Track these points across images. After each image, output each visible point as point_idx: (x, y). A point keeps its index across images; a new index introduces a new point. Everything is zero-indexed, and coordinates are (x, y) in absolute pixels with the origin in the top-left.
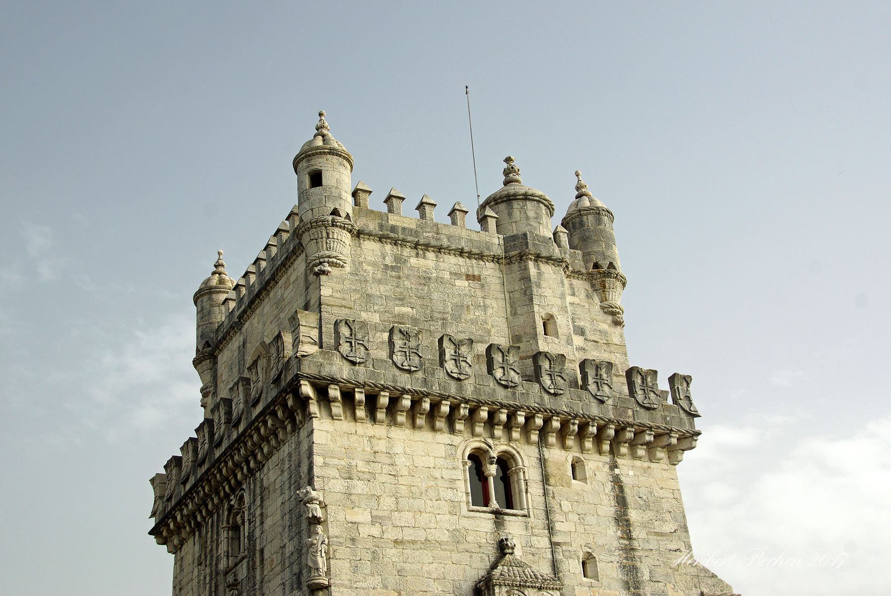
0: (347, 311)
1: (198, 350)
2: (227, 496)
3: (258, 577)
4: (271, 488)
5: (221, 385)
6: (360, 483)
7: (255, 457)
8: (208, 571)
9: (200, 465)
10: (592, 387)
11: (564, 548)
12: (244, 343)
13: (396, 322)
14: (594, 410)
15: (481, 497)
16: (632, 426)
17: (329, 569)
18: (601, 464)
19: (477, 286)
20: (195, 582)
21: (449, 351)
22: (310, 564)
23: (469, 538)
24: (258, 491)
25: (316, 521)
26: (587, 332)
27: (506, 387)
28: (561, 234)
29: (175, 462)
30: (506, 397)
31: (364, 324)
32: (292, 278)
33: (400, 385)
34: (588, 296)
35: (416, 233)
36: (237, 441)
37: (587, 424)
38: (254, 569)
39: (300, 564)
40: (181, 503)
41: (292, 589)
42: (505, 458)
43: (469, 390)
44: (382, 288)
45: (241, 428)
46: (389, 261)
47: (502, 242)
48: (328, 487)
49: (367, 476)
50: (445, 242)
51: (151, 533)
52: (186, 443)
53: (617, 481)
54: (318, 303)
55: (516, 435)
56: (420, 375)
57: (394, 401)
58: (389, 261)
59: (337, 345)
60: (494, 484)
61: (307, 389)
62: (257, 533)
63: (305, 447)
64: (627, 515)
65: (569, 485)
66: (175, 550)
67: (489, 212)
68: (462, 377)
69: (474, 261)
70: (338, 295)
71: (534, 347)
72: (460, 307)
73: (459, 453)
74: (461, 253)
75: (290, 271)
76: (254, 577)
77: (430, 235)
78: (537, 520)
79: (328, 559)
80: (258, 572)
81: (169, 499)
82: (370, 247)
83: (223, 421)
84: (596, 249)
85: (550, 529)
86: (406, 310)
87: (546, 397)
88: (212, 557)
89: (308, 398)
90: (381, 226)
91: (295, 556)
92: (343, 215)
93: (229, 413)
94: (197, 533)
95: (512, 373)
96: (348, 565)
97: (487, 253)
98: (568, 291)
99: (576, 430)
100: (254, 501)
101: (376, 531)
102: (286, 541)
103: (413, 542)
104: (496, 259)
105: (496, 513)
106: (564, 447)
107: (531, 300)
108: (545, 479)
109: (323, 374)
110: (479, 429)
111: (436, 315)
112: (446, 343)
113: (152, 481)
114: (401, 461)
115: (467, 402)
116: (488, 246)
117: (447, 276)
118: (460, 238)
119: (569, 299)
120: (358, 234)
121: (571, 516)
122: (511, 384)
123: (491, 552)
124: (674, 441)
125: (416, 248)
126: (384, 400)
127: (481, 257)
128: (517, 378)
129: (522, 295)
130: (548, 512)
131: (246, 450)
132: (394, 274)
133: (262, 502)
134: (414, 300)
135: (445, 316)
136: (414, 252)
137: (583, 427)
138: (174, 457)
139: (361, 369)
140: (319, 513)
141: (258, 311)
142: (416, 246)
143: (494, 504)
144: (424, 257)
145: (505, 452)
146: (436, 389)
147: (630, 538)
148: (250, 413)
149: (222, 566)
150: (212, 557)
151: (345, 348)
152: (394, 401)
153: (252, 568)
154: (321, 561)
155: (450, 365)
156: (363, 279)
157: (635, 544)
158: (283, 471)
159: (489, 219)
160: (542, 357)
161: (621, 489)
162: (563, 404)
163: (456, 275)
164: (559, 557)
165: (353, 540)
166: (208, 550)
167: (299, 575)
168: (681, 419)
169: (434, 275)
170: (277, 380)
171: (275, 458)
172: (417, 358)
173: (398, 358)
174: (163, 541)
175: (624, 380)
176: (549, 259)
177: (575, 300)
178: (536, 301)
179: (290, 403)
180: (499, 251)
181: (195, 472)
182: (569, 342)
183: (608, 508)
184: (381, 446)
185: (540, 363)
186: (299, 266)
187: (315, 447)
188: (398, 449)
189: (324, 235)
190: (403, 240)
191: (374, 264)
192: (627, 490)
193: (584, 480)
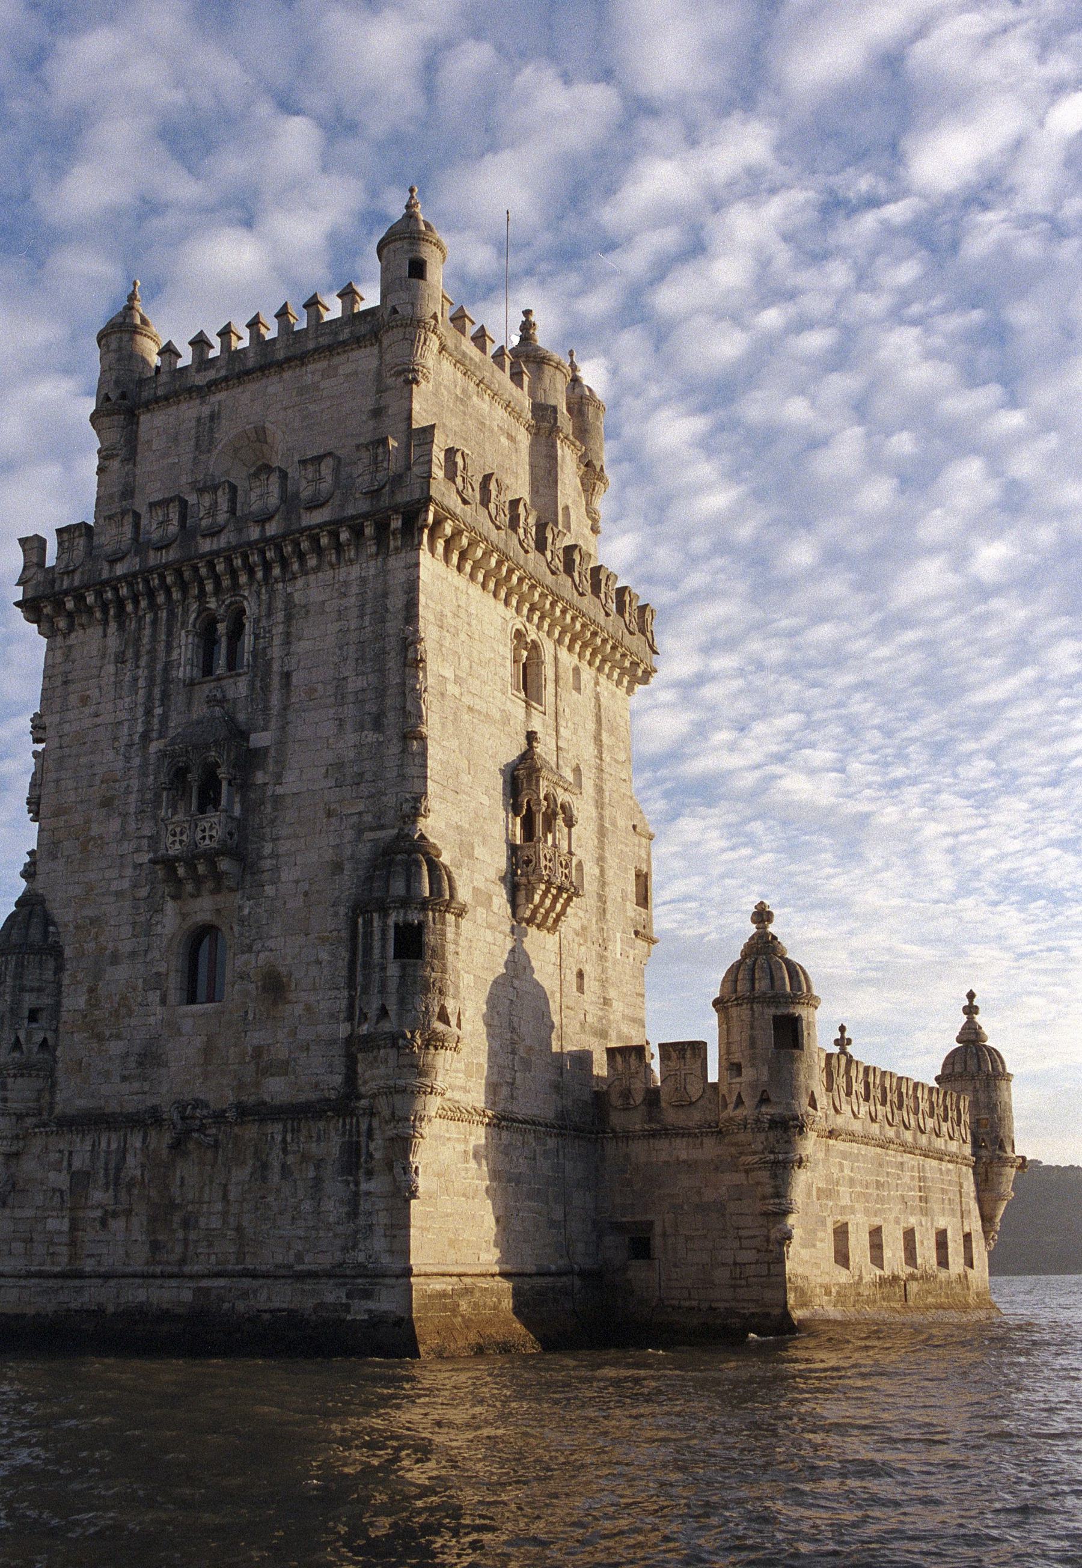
7: (284, 563)
9: (159, 549)
12: (213, 417)
22: (409, 707)
24: (279, 604)
27: (553, 573)
38: (266, 689)
41: (362, 728)
45: (272, 529)
54: (405, 415)
62: (276, 652)
63: (399, 577)
75: (336, 360)
76: (266, 700)
78: (552, 722)
83: (224, 506)
85: (557, 731)
87: (576, 594)
88: (153, 660)
94: (113, 626)
100: (269, 614)
103: (480, 713)
106: (570, 649)
107: (556, 482)
113: (23, 542)
114: (474, 622)
123: (523, 741)
124: (640, 673)
125: (478, 385)
133: (289, 618)
150: (153, 660)
153: (260, 689)
160: (577, 551)
165: (442, 694)
166: (143, 650)
171: (327, 575)
179: (396, 523)
188: (473, 610)
193: (578, 689)
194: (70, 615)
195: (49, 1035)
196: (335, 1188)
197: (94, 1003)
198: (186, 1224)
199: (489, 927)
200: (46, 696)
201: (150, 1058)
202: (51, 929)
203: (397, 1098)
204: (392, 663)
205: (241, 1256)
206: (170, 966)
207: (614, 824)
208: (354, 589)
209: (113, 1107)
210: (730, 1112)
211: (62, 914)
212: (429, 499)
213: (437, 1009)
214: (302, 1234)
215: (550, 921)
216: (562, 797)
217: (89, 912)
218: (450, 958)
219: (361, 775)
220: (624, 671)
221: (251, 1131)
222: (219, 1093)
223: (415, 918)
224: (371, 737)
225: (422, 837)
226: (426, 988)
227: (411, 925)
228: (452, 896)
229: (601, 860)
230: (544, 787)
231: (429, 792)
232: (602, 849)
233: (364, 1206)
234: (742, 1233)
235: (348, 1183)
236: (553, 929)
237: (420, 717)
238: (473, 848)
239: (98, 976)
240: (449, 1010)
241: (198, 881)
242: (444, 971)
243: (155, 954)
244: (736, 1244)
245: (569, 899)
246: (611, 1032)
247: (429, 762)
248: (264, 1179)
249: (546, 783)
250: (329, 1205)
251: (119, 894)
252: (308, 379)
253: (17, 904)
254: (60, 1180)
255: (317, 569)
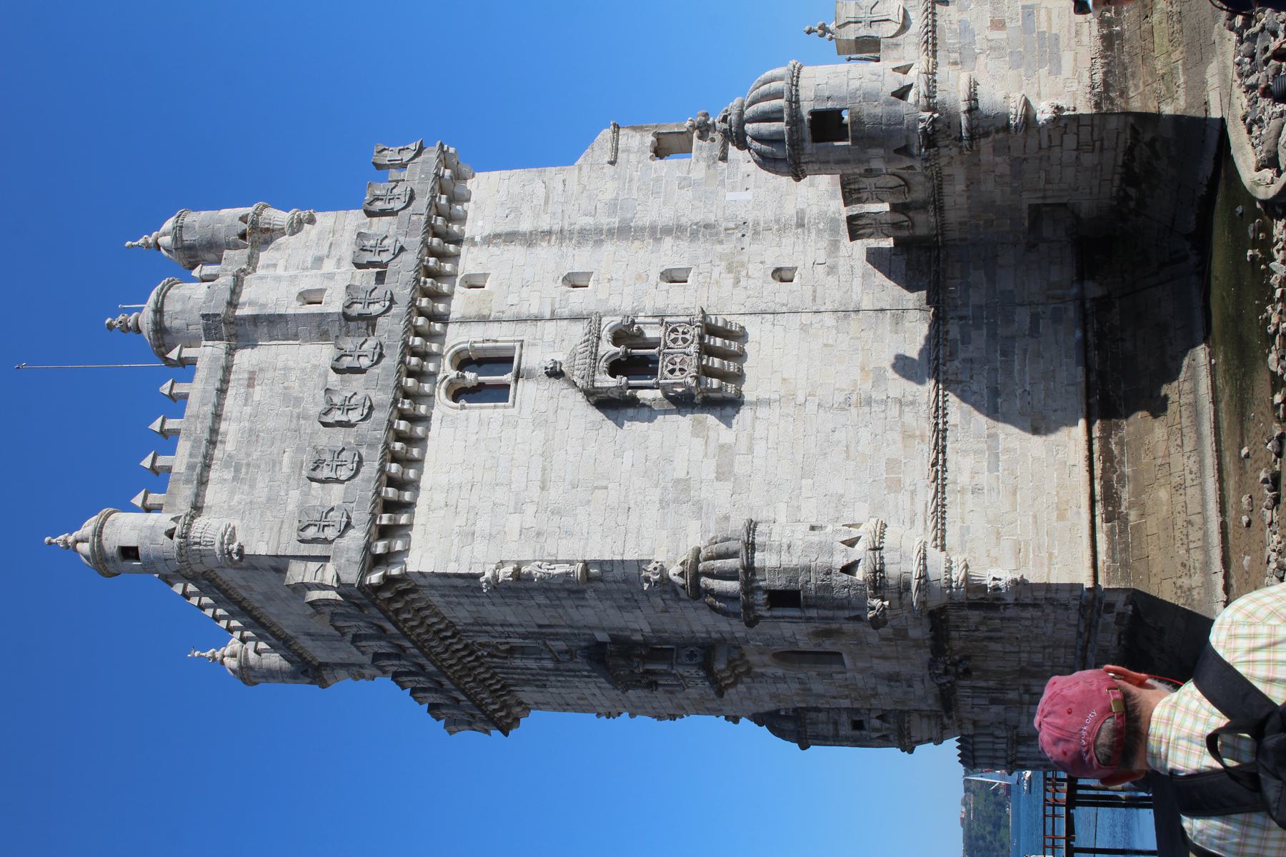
0: (285, 526)
1: (311, 683)
2: (477, 658)
3: (567, 631)
4: (476, 615)
5: (353, 660)
6: (479, 524)
7: (440, 630)
8: (553, 678)
9: (442, 685)
10: (384, 257)
11: (557, 306)
13: (300, 474)
14: (410, 259)
15: (499, 393)
16: (429, 218)
17: (567, 562)
18: (469, 256)
19: (261, 376)
20: (563, 691)
21: (337, 416)
22: (561, 581)
23: (543, 408)
24: (477, 628)
25: (517, 574)
26: (319, 254)
27: (381, 356)
28: (203, 273)
29: (433, 709)
30: (392, 356)
31: (303, 510)
32: (243, 583)
33: (375, 475)
34: (278, 249)
35: (196, 442)
36: (421, 649)
37: (425, 267)
38: (557, 634)
39: (558, 590)
40: (479, 706)
42: (458, 362)
43: (383, 397)
44: (260, 485)
45: (408, 644)
46: (228, 475)
47: (210, 343)
48: (484, 558)
49: (472, 516)
50: (209, 409)
51: (506, 734)
52: (416, 698)
53: (490, 240)
55: (434, 347)
56: (364, 451)
57: (392, 482)
58: (228, 475)
59: (326, 541)
60: (486, 376)
61: (375, 578)
63: (436, 581)
64: (525, 234)
65: (490, 293)
66: (527, 709)
67: (173, 355)
68: (368, 404)
69: (232, 377)
70: (266, 535)
71: (336, 317)
72: (289, 398)
73: (451, 412)
74: (222, 392)
75: (232, 584)
76: (566, 634)
77: (199, 426)
78: (526, 332)
79: (557, 562)
80: (561, 630)
81: (473, 716)
82: (212, 495)
84: (222, 235)
85: (537, 319)
86: (286, 459)
87: (393, 311)
89: (385, 577)
90: (188, 481)
91: (550, 594)
92: (173, 525)
93: (388, 656)
95: (365, 346)
96: (564, 541)
97: (222, 362)
98: (271, 272)
99: (432, 282)
101: (530, 509)
102: (533, 603)
103: (544, 469)
104: (230, 352)
105: (518, 376)
106: (447, 297)
108: (483, 319)
109: (358, 558)
110: (427, 387)
111: (293, 425)
112: (329, 419)
113: (451, 733)
115: (395, 401)
116: (215, 359)
117: (248, 410)
118: (204, 391)
119: (280, 271)
120: (197, 508)
121: (524, 295)
122: (378, 350)
123: (557, 384)
124: (448, 173)
126: (391, 493)
127: (227, 369)
128: (371, 342)
129: (273, 325)
130: (519, 320)
131: (432, 640)
132: (244, 470)
133: (486, 625)
134: (275, 450)
135: (295, 415)
136: (218, 445)
137: (430, 273)
138: (429, 710)
139: (353, 516)
140: (509, 569)
141: (274, 620)
142: (212, 443)
143: (508, 378)
144: (226, 434)
145: (452, 361)
146: (381, 434)
147: (550, 233)
148: (392, 636)
149: (549, 664)
151: (330, 533)
152: (392, 482)
153: (556, 637)
154: (560, 569)
155: (354, 416)
156: (248, 507)
157: (556, 228)
158: (459, 603)
159: (183, 355)
160: (349, 311)
161: (497, 236)
162: (404, 294)
163: (247, 399)
164: (566, 313)
165: (539, 534)
167: (570, 592)
168: (424, 162)
169: (247, 424)
170: (360, 607)
171: (445, 612)
172: (344, 453)
173: (344, 473)
174: (517, 720)
175: (375, 220)
176: (235, 291)
177: (281, 263)
178: (282, 311)
179: (388, 595)
180: (221, 346)
181: (449, 691)
182: (330, 276)
183: (516, 252)
184: (440, 498)
185: (355, 314)
186: (230, 577)
187: (438, 570)
189: (195, 547)
190: (205, 457)
191: (232, 493)
192: (498, 231)
193: (485, 276)
194: (510, 706)
195: (874, 715)
196: (1010, 613)
197: (847, 697)
198: (1040, 665)
199: (751, 450)
200: (584, 711)
201: (892, 678)
202: (783, 713)
203: (929, 604)
204: (520, 585)
205: (1066, 647)
206: (810, 673)
207: (613, 206)
208: (454, 599)
209: (937, 690)
210: (919, 170)
211: (769, 706)
212: (362, 587)
213: (845, 577)
214: (1050, 626)
215: (734, 346)
216: (607, 348)
217: (767, 698)
218: (794, 560)
219: (627, 599)
220: (453, 200)
221: (957, 645)
222: (926, 655)
223: (761, 598)
224: (590, 594)
225: (681, 574)
226: (828, 587)
227: (768, 599)
228: (734, 555)
229: (657, 233)
230: (606, 381)
231: (635, 557)
232: (643, 229)
233: (1028, 601)
234: (1045, 145)
235: (1005, 609)
236: (741, 336)
237: (567, 574)
238: (678, 481)
239: (823, 696)
240: (845, 562)
241: (735, 668)
242: (808, 569)
243: (801, 676)
244: (1057, 150)
245: (712, 330)
246: (830, 214)
247: (607, 558)
248: (1001, 638)
249: (597, 377)
250: (1024, 614)
251: (749, 689)
252: (261, 597)
253: (760, 725)
254: (995, 709)
255: (437, 614)
